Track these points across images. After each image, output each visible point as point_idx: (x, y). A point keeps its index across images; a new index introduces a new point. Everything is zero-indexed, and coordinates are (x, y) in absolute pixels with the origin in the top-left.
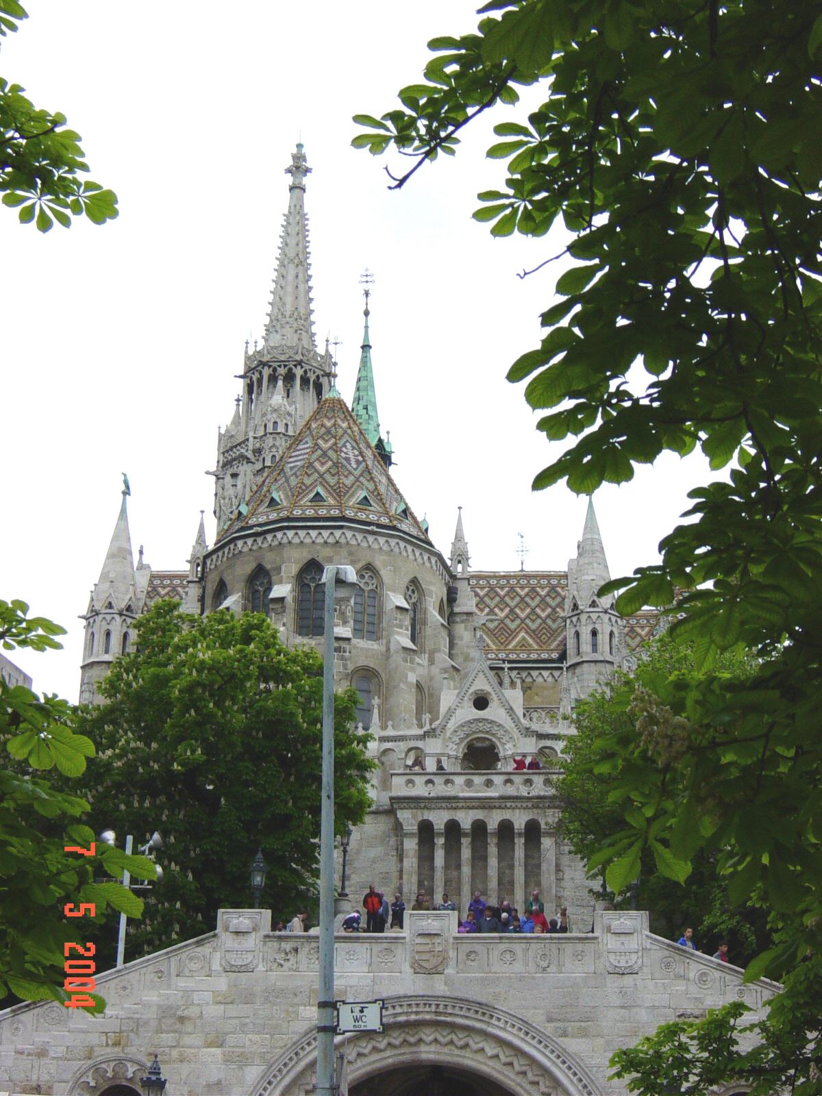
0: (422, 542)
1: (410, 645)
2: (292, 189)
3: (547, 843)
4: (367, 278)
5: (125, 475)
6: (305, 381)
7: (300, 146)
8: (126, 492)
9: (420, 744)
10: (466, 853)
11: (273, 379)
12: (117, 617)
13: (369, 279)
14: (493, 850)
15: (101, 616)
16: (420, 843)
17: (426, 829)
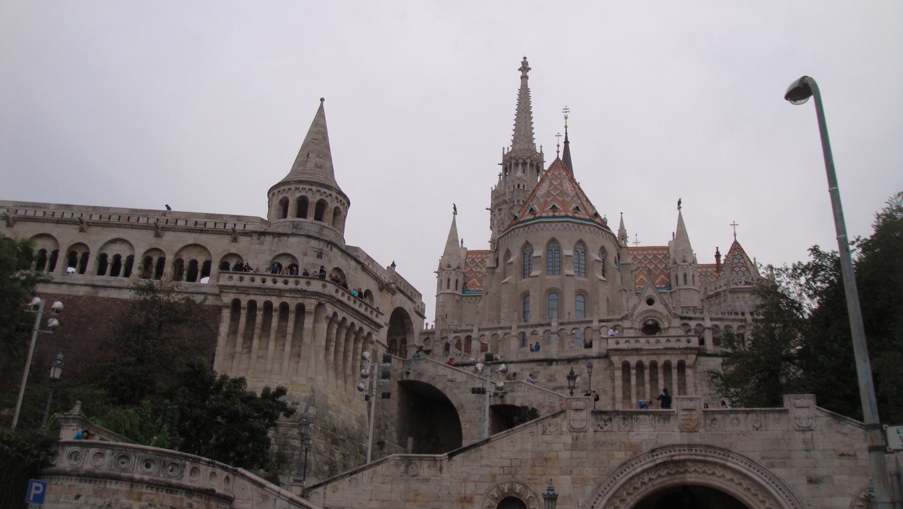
1: (603, 278)
2: (522, 78)
3: (689, 372)
4: (566, 110)
5: (455, 205)
6: (531, 165)
7: (525, 58)
8: (455, 213)
9: (620, 323)
10: (647, 377)
11: (517, 164)
12: (453, 272)
13: (567, 110)
14: (661, 375)
15: (445, 272)
16: (623, 373)
17: (626, 367)
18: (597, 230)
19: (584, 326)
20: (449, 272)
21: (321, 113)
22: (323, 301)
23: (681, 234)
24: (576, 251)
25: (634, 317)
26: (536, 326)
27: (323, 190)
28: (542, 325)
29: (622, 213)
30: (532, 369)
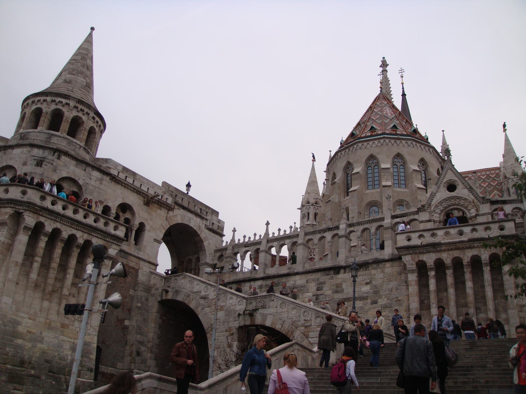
0: (424, 141)
5: (313, 154)
7: (384, 58)
8: (314, 160)
9: (416, 217)
10: (450, 280)
12: (311, 207)
13: (402, 71)
14: (468, 276)
15: (305, 207)
17: (422, 267)
18: (414, 143)
19: (375, 225)
20: (308, 207)
21: (89, 40)
22: (21, 209)
23: (509, 151)
24: (394, 164)
25: (432, 208)
26: (324, 231)
27: (58, 99)
28: (330, 229)
29: (443, 131)
30: (318, 279)
